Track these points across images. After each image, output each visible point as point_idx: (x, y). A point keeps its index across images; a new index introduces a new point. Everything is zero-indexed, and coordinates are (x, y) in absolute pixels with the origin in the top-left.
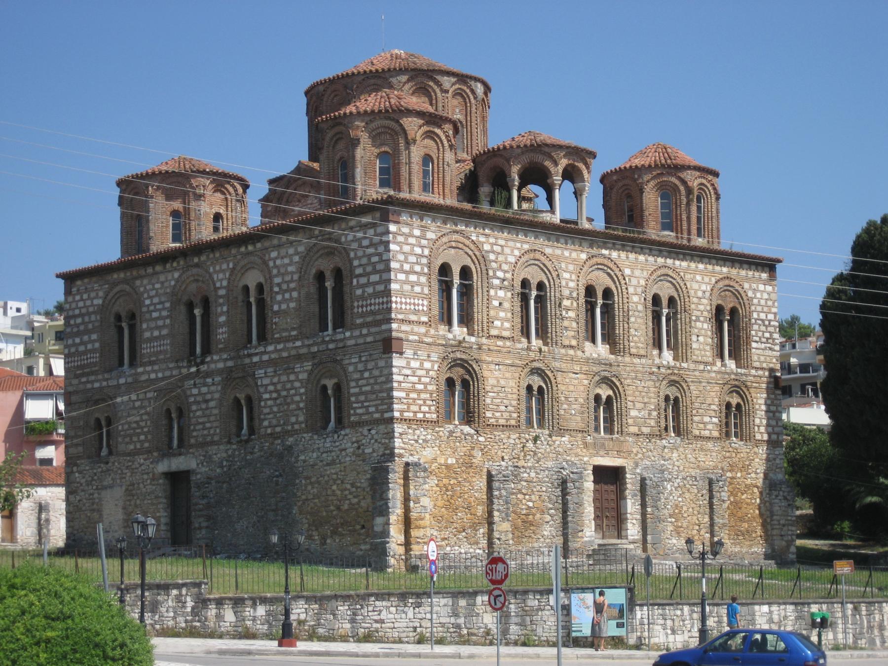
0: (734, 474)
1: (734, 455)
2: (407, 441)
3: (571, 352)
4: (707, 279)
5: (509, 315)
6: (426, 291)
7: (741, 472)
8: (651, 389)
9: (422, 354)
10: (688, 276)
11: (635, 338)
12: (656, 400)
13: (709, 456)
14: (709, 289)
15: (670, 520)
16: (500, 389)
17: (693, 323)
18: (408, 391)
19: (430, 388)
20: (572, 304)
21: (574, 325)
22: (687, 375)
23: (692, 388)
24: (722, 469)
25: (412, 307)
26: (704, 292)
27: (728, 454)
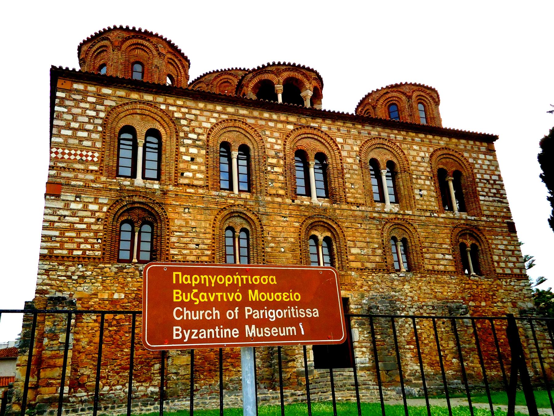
0: (477, 303)
1: (475, 287)
2: (56, 277)
3: (279, 200)
4: (425, 149)
5: (203, 168)
6: (99, 145)
7: (485, 301)
8: (373, 231)
9: (86, 198)
10: (404, 146)
11: (352, 190)
12: (380, 240)
13: (446, 288)
14: (427, 155)
15: (408, 347)
16: (190, 229)
17: (414, 181)
18: (63, 231)
19: (94, 227)
20: (278, 161)
21: (281, 178)
22: (413, 220)
23: (418, 230)
24: (463, 298)
25: (78, 158)
26: (423, 158)
27: (467, 286)
